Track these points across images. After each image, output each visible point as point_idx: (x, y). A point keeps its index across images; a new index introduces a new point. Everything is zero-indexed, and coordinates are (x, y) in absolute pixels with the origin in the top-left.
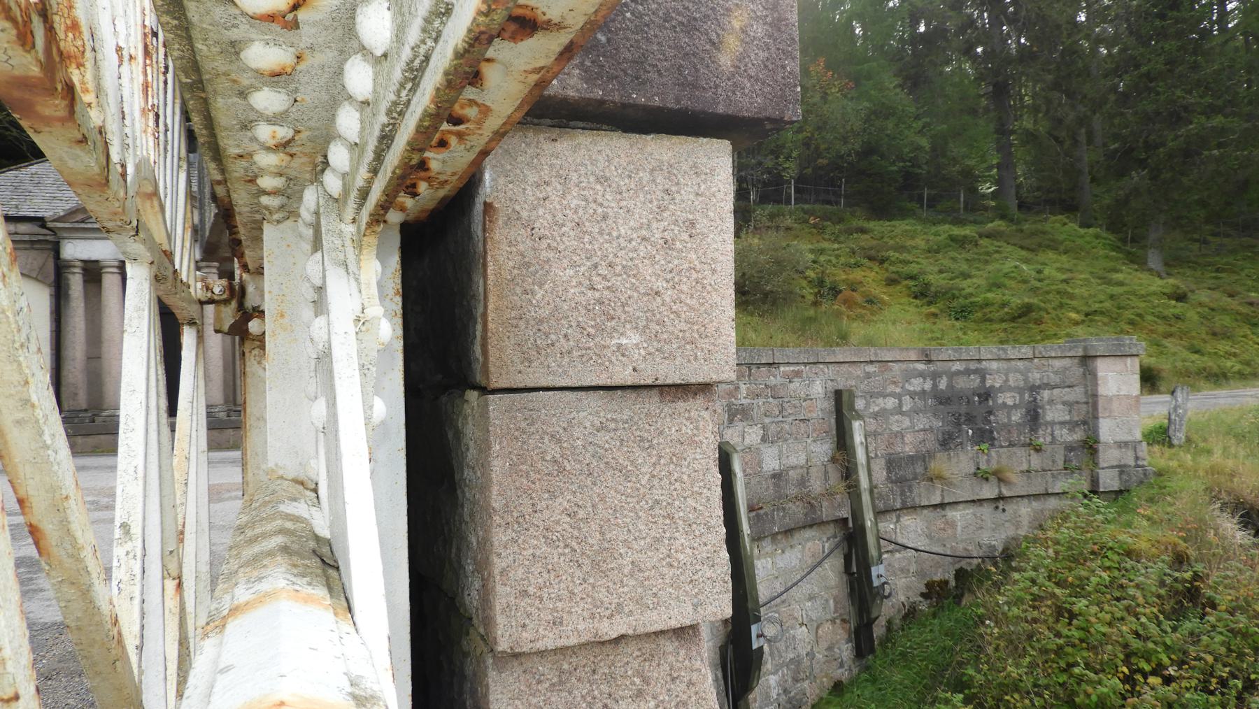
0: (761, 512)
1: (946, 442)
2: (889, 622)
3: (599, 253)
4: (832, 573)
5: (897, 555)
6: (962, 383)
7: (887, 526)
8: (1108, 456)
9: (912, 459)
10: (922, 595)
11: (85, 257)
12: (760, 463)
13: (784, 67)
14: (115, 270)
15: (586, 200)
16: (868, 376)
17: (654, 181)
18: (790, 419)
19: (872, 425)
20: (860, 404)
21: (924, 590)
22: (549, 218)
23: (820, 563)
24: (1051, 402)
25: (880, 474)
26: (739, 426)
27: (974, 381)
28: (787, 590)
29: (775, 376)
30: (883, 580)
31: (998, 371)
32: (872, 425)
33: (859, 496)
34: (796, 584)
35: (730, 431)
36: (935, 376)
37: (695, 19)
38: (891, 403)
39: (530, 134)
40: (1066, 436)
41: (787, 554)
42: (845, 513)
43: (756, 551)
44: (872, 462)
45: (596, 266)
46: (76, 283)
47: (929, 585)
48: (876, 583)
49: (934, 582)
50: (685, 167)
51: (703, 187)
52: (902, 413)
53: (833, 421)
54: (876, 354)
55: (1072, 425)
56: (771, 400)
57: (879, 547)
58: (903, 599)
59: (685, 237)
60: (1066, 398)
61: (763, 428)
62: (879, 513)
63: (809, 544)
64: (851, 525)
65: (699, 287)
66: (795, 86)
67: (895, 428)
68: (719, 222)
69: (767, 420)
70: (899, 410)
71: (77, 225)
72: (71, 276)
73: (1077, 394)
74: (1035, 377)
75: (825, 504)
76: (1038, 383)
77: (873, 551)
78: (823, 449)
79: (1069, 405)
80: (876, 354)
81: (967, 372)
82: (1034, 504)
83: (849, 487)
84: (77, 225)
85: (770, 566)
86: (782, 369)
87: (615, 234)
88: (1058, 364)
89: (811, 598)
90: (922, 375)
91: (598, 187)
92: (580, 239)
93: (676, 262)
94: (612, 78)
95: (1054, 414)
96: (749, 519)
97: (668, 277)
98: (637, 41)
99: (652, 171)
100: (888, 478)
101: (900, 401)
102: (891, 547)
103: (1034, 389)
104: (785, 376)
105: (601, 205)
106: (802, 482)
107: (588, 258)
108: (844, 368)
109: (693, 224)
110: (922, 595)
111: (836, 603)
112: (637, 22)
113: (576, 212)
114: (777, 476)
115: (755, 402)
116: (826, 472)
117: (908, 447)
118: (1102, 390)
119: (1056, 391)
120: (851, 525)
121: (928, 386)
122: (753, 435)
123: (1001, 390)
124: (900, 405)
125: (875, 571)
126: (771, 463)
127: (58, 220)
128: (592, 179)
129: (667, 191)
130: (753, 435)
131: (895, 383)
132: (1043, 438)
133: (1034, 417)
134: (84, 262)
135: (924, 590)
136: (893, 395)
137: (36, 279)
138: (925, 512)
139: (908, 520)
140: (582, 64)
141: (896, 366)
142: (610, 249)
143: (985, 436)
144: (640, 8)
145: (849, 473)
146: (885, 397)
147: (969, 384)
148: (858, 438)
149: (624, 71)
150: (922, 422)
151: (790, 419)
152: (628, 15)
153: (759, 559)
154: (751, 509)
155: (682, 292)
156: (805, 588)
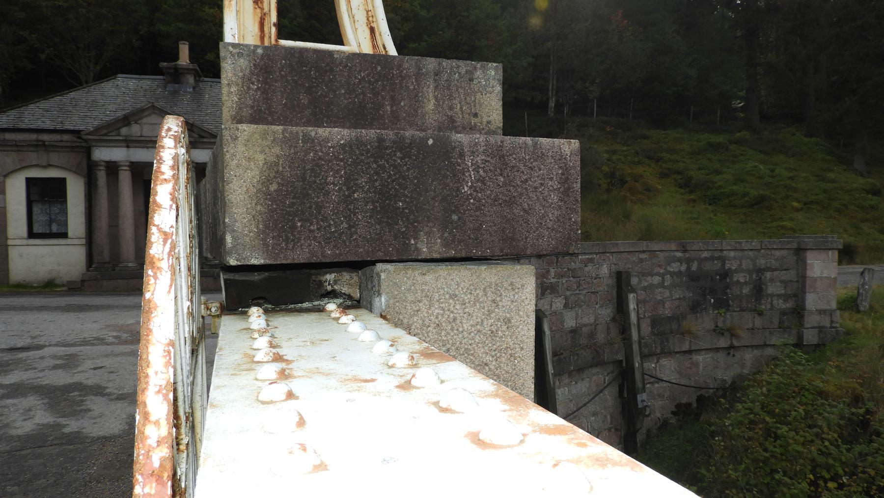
0: (562, 357)
1: (695, 307)
2: (649, 431)
3: (451, 342)
4: (609, 397)
5: (657, 385)
6: (708, 266)
7: (650, 365)
8: (811, 320)
9: (670, 319)
10: (673, 413)
11: (107, 158)
12: (562, 322)
13: (570, 219)
15: (443, 309)
16: (641, 261)
17: (486, 295)
18: (584, 292)
19: (643, 295)
20: (634, 281)
21: (674, 409)
22: (421, 322)
23: (601, 391)
24: (772, 280)
25: (646, 329)
26: (549, 297)
27: (717, 265)
28: (578, 410)
29: (575, 263)
30: (645, 404)
31: (735, 258)
32: (643, 295)
33: (631, 346)
34: (585, 405)
35: (542, 301)
36: (689, 261)
37: (514, 197)
38: (656, 280)
39: (410, 272)
40: (781, 304)
41: (579, 384)
42: (620, 357)
43: (557, 383)
44: (641, 321)
45: (448, 350)
46: (102, 177)
47: (679, 406)
48: (640, 406)
49: (681, 404)
50: (505, 285)
51: (516, 296)
52: (664, 287)
53: (615, 293)
54: (647, 246)
55: (786, 297)
56: (571, 279)
57: (643, 379)
58: (659, 415)
59: (504, 328)
60: (783, 278)
61: (566, 298)
62: (644, 357)
63: (595, 378)
64: (624, 365)
65: (512, 359)
66: (577, 230)
67: (659, 297)
68: (526, 318)
69: (568, 293)
70: (662, 285)
73: (791, 275)
74: (761, 262)
75: (607, 351)
76: (763, 267)
77: (639, 384)
78: (606, 313)
79: (785, 283)
80: (647, 246)
81: (712, 258)
82: (756, 352)
83: (624, 339)
85: (566, 393)
86: (580, 257)
87: (461, 329)
88: (778, 253)
89: (595, 414)
90: (679, 260)
91: (451, 301)
92: (439, 334)
93: (498, 344)
94: (460, 242)
95: (773, 289)
96: (553, 362)
97: (493, 353)
98: (478, 216)
99: (485, 289)
100: (652, 333)
101: (663, 278)
102: (652, 380)
103: (760, 271)
104: (582, 261)
105: (452, 312)
106: (592, 335)
107: (443, 346)
108: (624, 256)
109: (509, 321)
110: (673, 413)
111: (612, 417)
112: (477, 204)
113: (437, 318)
114: (574, 331)
115: (560, 281)
116: (608, 329)
117: (667, 311)
118: (809, 273)
119: (776, 273)
120: (624, 365)
121: (683, 268)
122: (558, 304)
123: (736, 271)
124: (663, 281)
125: (639, 398)
126: (570, 322)
127: (90, 133)
128: (447, 296)
129: (494, 301)
130: (558, 304)
131: (659, 266)
132: (764, 306)
133: (759, 290)
134: (107, 162)
135: (674, 409)
136: (658, 274)
137: (75, 172)
138: (678, 355)
139: (664, 361)
140: (442, 236)
141: (661, 255)
142: (458, 338)
143: (723, 304)
144: (480, 195)
145: (624, 330)
146: (652, 276)
147: (712, 267)
148: (632, 306)
149: (469, 236)
150: (678, 293)
151: (584, 292)
152: (472, 201)
153: (559, 388)
154: (555, 354)
155: (501, 362)
156: (591, 407)
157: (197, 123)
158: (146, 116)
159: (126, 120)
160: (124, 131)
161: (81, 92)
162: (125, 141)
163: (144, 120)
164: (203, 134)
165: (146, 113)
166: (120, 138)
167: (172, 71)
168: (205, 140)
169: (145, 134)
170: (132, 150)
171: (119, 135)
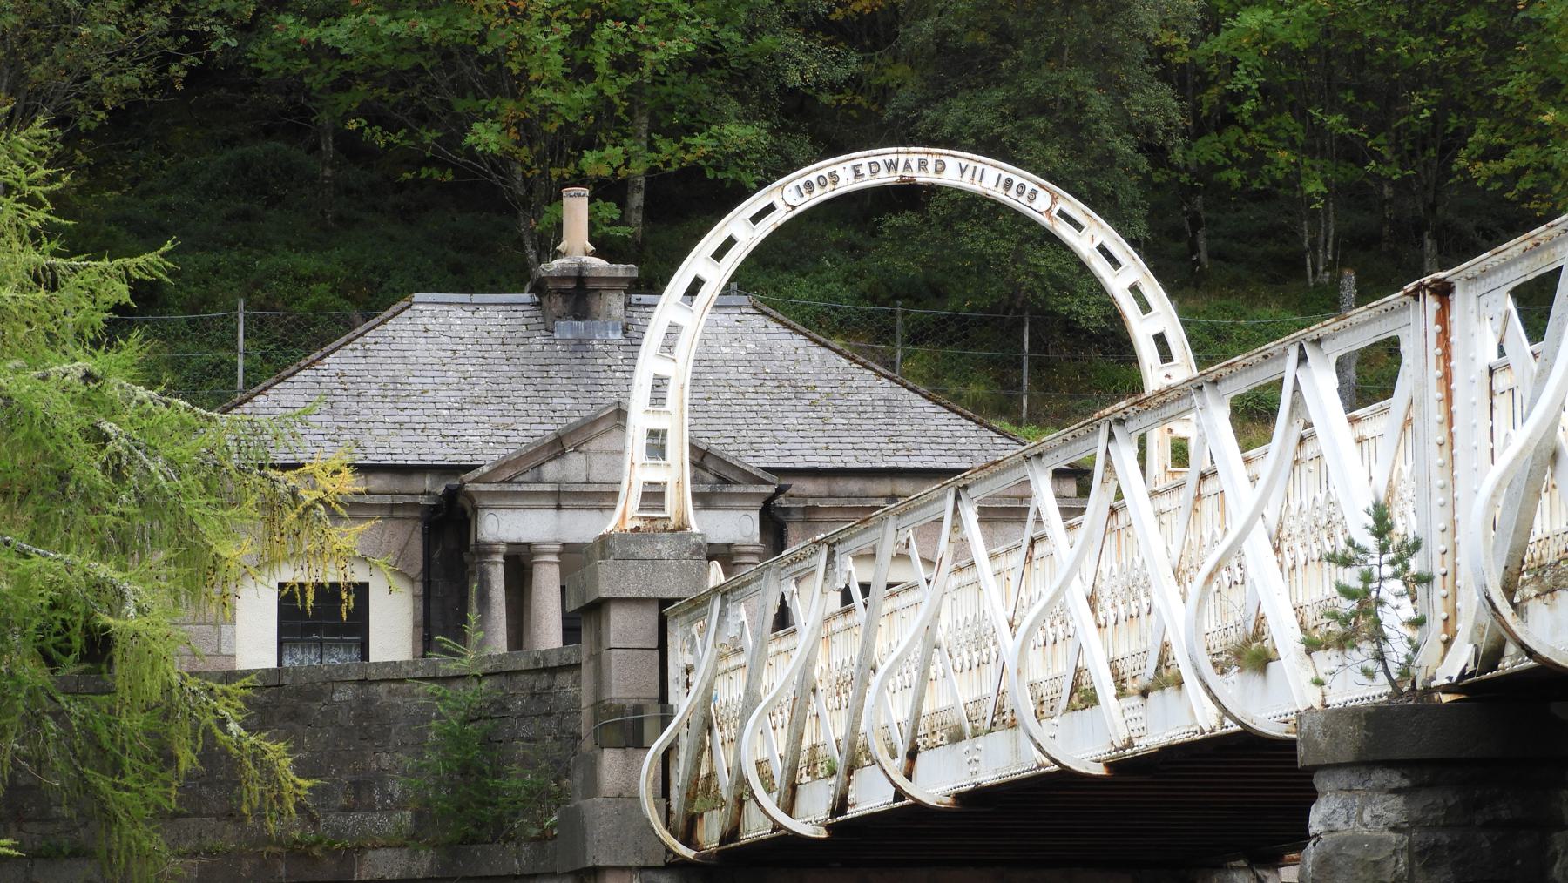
11: (513, 537)
14: (554, 558)
71: (506, 487)
72: (491, 568)
84: (506, 487)
134: (508, 544)
157: (717, 449)
158: (599, 435)
159: (558, 447)
160: (551, 470)
161: (347, 351)
163: (595, 445)
165: (601, 427)
166: (547, 488)
167: (570, 285)
168: (735, 489)
169: (595, 477)
170: (566, 514)
171: (539, 481)
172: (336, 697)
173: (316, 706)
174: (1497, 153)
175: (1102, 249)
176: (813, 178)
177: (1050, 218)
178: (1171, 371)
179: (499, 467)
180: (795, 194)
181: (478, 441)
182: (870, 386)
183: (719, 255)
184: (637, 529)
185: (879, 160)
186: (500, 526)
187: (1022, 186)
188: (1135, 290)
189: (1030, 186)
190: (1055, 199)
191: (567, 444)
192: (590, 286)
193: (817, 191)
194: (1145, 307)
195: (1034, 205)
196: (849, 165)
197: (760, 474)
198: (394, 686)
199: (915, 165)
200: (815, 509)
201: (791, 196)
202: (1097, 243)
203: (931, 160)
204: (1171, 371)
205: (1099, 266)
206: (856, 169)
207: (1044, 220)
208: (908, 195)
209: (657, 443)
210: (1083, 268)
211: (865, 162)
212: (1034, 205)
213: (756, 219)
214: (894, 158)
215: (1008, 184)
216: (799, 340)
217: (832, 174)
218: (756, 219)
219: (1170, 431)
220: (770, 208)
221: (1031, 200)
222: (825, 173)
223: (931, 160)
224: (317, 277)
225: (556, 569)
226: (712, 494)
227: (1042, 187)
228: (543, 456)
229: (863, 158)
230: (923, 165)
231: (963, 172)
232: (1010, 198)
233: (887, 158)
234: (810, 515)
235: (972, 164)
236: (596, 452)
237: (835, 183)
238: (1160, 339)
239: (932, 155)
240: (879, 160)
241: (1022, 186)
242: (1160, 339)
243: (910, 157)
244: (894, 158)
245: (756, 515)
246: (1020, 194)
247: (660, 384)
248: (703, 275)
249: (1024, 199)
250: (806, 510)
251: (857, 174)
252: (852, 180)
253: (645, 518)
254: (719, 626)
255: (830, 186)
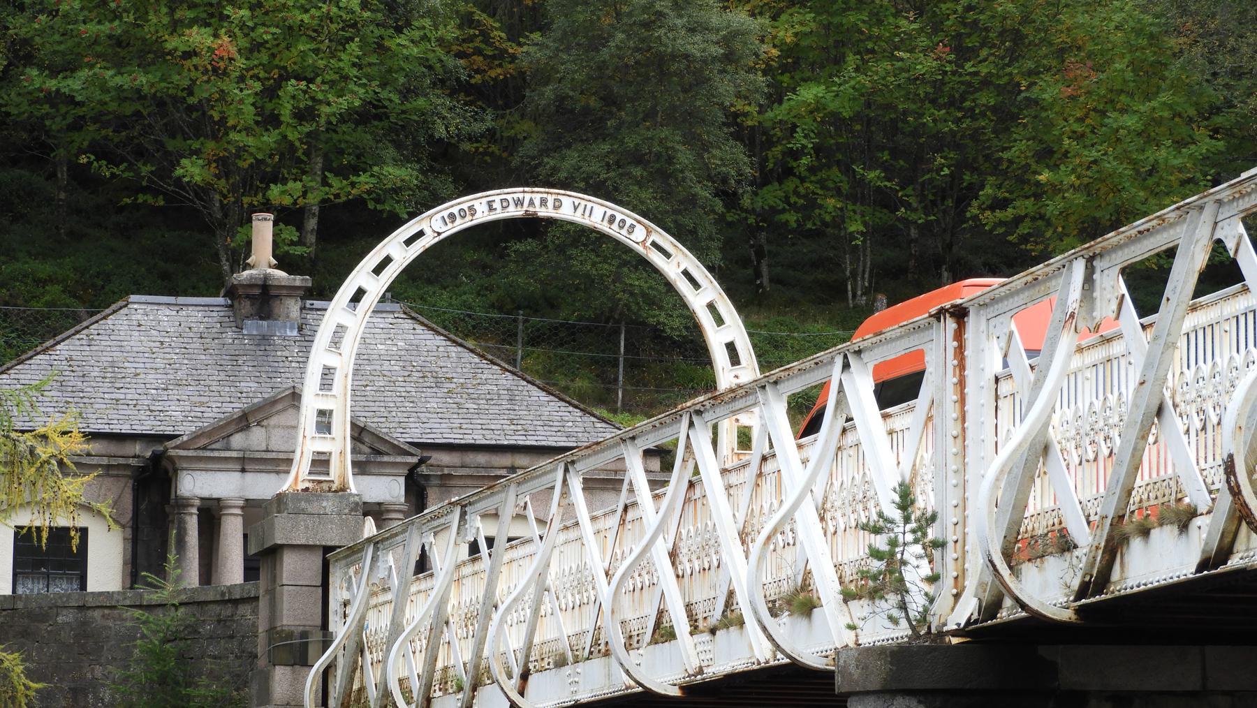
11: (205, 493)
14: (238, 511)
71: (201, 453)
72: (188, 518)
84: (201, 453)
127: (182, 446)
134: (202, 499)
157: (372, 426)
158: (278, 412)
159: (244, 421)
160: (238, 440)
161: (74, 341)
162: (242, 460)
163: (273, 421)
164: (383, 448)
165: (279, 407)
166: (234, 454)
167: (257, 292)
168: (386, 459)
169: (274, 445)
170: (249, 476)
171: (228, 449)
172: (60, 619)
173: (43, 626)
174: (1002, 204)
175: (686, 273)
176: (455, 210)
177: (645, 247)
178: (738, 373)
179: (196, 437)
180: (440, 222)
181: (179, 415)
182: (497, 379)
183: (378, 270)
184: (307, 489)
185: (509, 197)
186: (196, 484)
187: (623, 221)
188: (711, 307)
189: (629, 222)
190: (649, 233)
191: (251, 419)
192: (273, 292)
193: (459, 221)
194: (719, 321)
195: (632, 237)
196: (484, 201)
197: (406, 447)
198: (107, 611)
199: (537, 202)
200: (450, 476)
201: (437, 225)
202: (682, 268)
203: (551, 199)
204: (738, 373)
205: (683, 287)
206: (490, 204)
207: (640, 249)
208: (531, 226)
209: (324, 421)
210: (670, 287)
211: (497, 199)
212: (632, 237)
213: (409, 242)
214: (521, 196)
215: (612, 219)
216: (439, 341)
217: (471, 208)
218: (409, 242)
219: (737, 420)
220: (421, 234)
221: (630, 233)
222: (465, 206)
223: (551, 199)
224: (51, 280)
225: (240, 520)
226: (368, 462)
227: (639, 222)
228: (232, 428)
229: (496, 195)
230: (544, 202)
231: (576, 208)
232: (613, 231)
233: (515, 196)
234: (446, 481)
235: (583, 203)
236: (274, 427)
237: (473, 215)
238: (731, 347)
239: (551, 195)
240: (509, 197)
241: (623, 221)
242: (731, 347)
243: (533, 196)
244: (521, 196)
245: (402, 480)
246: (621, 228)
247: (328, 373)
248: (365, 286)
249: (624, 232)
250: (443, 477)
251: (491, 209)
252: (486, 213)
253: (313, 481)
254: (371, 569)
255: (468, 218)
